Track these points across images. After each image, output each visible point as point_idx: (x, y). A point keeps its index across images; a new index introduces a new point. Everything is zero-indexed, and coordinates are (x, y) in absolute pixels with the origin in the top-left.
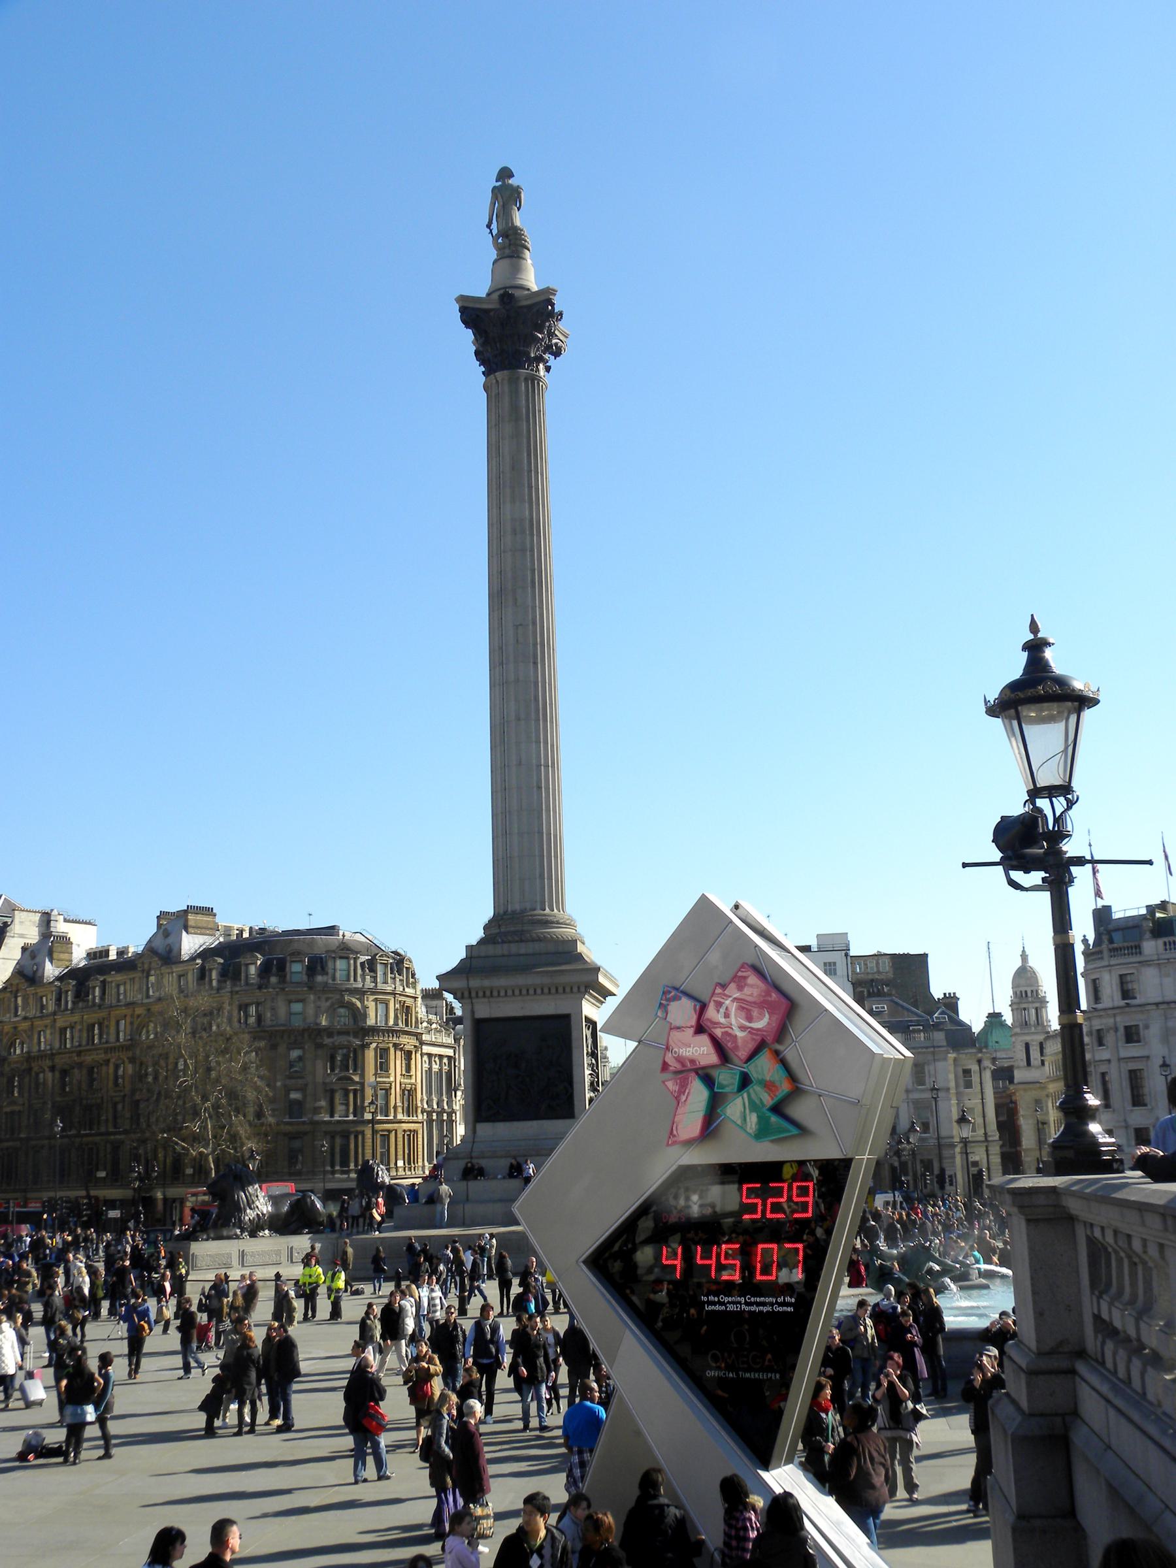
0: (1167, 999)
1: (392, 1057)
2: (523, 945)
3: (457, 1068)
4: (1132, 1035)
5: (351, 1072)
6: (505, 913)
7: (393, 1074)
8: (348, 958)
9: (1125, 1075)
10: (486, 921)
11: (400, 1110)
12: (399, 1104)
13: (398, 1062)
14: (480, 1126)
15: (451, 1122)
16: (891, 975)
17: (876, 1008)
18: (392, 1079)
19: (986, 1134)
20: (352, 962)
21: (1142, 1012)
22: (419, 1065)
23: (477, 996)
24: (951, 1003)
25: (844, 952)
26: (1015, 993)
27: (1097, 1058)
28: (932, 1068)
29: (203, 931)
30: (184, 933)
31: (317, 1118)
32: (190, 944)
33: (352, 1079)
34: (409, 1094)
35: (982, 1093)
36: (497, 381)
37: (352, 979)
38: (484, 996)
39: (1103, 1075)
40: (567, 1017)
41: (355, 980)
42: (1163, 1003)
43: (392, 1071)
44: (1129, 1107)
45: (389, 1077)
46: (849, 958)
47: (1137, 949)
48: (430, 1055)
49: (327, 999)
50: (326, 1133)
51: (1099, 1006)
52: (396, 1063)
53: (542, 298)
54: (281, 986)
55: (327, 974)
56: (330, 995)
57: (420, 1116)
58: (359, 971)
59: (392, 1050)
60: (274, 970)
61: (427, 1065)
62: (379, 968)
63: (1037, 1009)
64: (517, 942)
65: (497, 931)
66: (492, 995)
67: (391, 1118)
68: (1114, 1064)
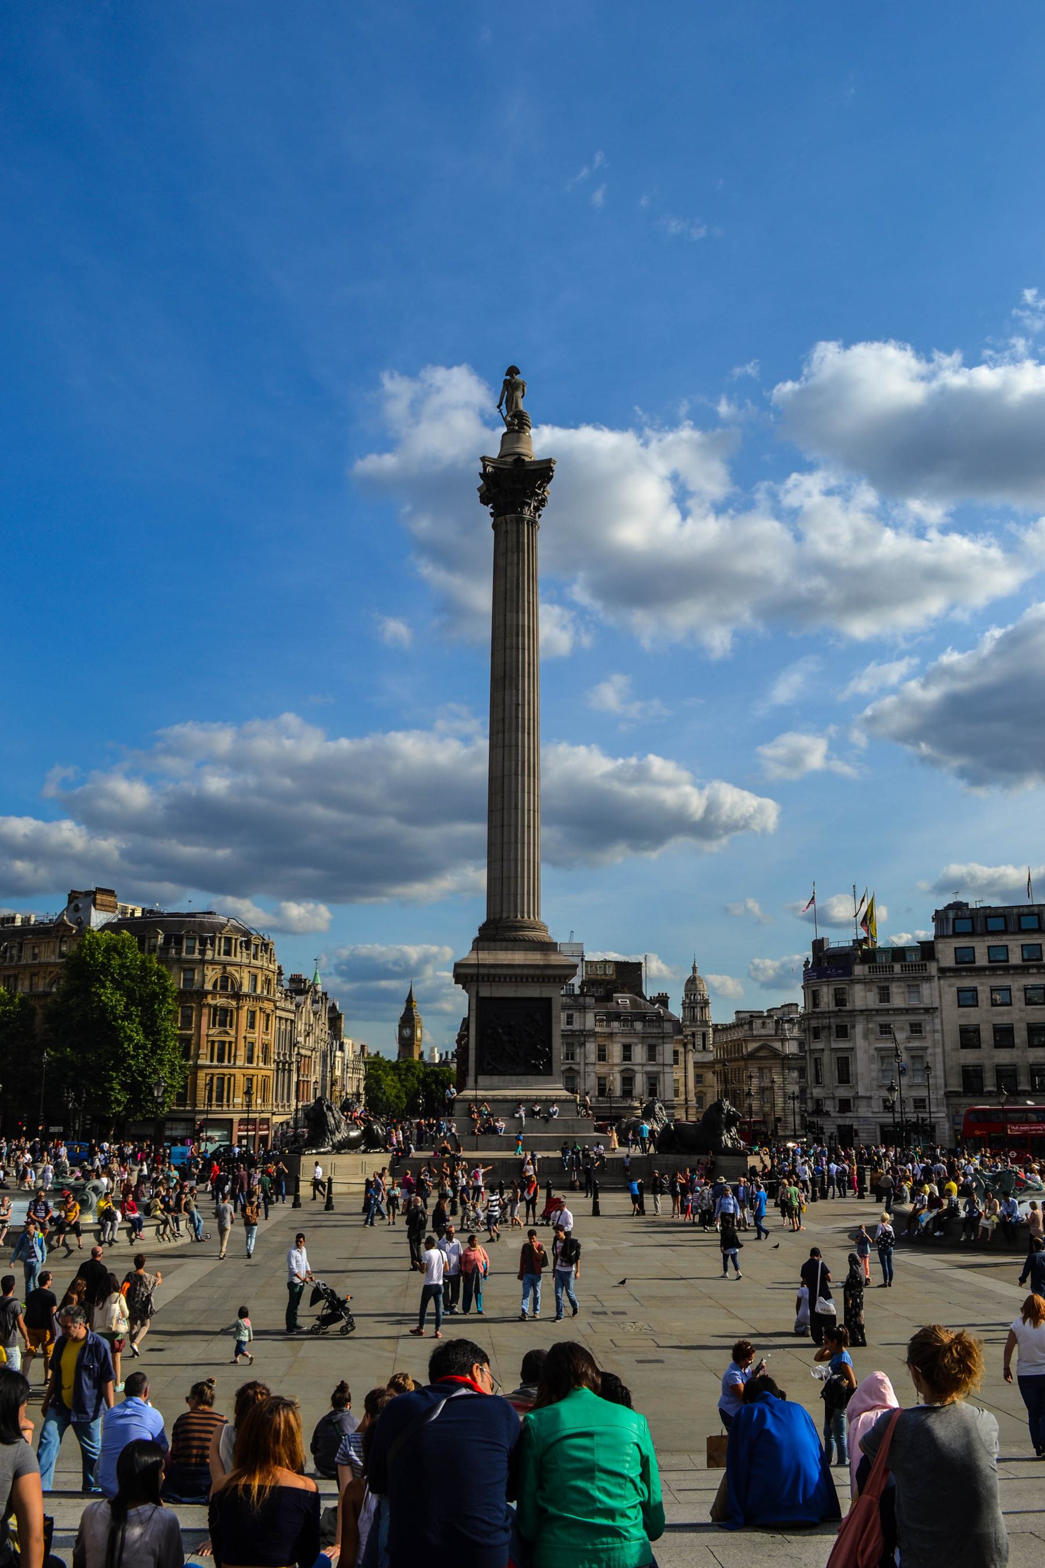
0: (869, 1007)
4: (843, 1032)
6: (501, 918)
9: (834, 1061)
10: (480, 924)
11: (260, 1059)
12: (260, 1055)
13: (262, 1022)
14: (480, 1078)
16: (614, 977)
18: (256, 1035)
19: (686, 1099)
20: (233, 941)
21: (850, 1016)
22: (274, 1023)
23: (483, 981)
24: (663, 1000)
26: (687, 995)
27: (812, 1048)
28: (661, 1048)
29: (107, 908)
30: (93, 909)
31: (200, 1062)
32: (98, 918)
33: (228, 1033)
34: (266, 1048)
35: (686, 1068)
36: (506, 522)
39: (816, 1059)
40: (549, 1000)
41: (235, 956)
42: (866, 1010)
43: (257, 1029)
44: (837, 1084)
45: (254, 1033)
47: (849, 972)
48: (280, 1018)
50: (207, 1075)
51: (818, 1010)
53: (547, 465)
57: (273, 1066)
58: (238, 949)
60: (173, 944)
61: (278, 1026)
62: (253, 947)
63: (702, 1008)
67: (255, 1065)
68: (826, 1053)
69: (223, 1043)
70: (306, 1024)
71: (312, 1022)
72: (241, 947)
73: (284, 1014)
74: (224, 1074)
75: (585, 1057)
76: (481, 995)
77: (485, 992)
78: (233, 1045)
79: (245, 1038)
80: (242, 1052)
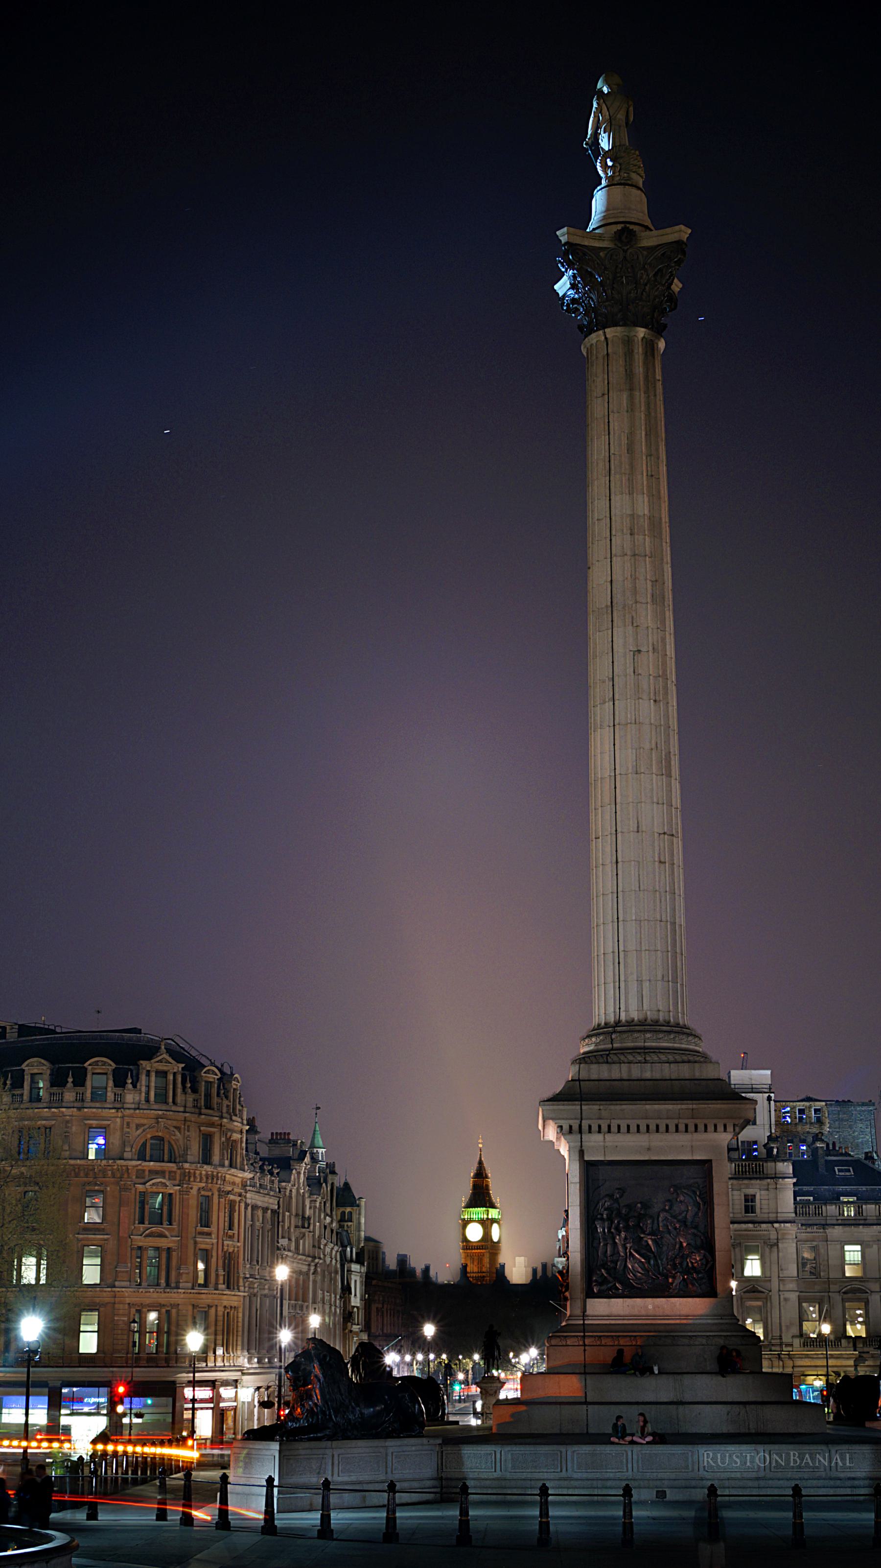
11: (221, 1279)
12: (221, 1272)
13: (222, 1214)
14: (591, 1302)
17: (839, 1171)
20: (171, 1077)
23: (590, 1131)
25: (767, 1095)
37: (171, 1100)
43: (214, 1229)
45: (209, 1234)
46: (772, 1103)
61: (249, 1223)
64: (640, 1062)
66: (609, 1131)
72: (184, 1087)
75: (780, 1269)
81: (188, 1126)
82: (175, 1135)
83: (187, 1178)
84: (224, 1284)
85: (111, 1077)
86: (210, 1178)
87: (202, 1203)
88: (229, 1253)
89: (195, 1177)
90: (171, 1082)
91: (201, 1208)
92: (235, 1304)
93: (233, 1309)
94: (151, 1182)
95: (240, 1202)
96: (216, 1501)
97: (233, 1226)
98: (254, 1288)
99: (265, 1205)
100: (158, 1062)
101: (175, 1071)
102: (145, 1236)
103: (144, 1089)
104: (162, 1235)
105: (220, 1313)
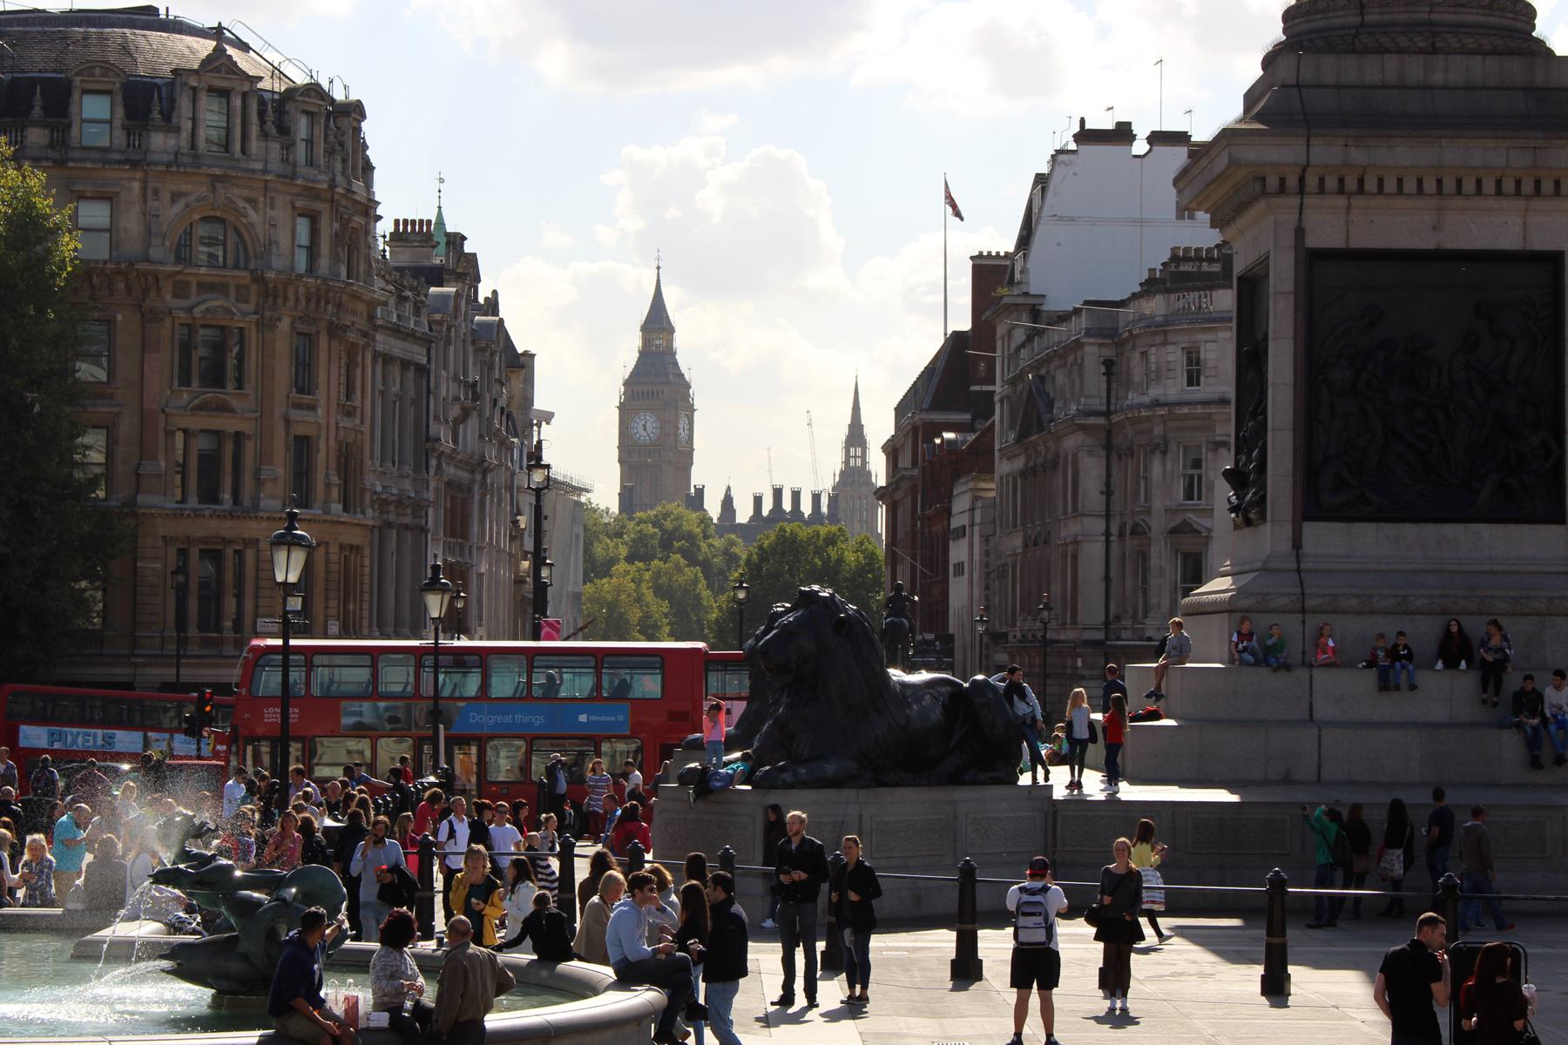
1: (323, 357)
2: (1439, 60)
3: (431, 397)
5: (230, 387)
7: (323, 402)
8: (224, 93)
11: (335, 493)
12: (335, 479)
14: (1311, 530)
15: (423, 530)
22: (369, 375)
23: (1322, 190)
34: (348, 462)
37: (237, 146)
38: (1341, 191)
43: (321, 396)
45: (312, 407)
48: (387, 359)
49: (175, 197)
52: (328, 376)
54: (56, 155)
55: (178, 130)
56: (183, 188)
58: (254, 129)
59: (323, 342)
60: (37, 112)
61: (379, 385)
62: (302, 126)
64: (1422, 51)
65: (1356, 20)
66: (1361, 190)
69: (217, 434)
70: (456, 378)
71: (473, 376)
72: (262, 122)
73: (397, 347)
74: (226, 542)
76: (1314, 241)
77: (1327, 231)
78: (249, 448)
79: (287, 421)
80: (279, 469)
81: (272, 199)
82: (246, 216)
83: (271, 299)
84: (339, 502)
85: (119, 99)
86: (313, 300)
87: (297, 349)
88: (347, 444)
89: (286, 298)
90: (239, 111)
91: (297, 359)
92: (357, 541)
93: (354, 553)
94: (203, 307)
95: (364, 349)
96: (711, 908)
97: (354, 392)
98: (388, 513)
99: (407, 357)
100: (209, 71)
101: (246, 89)
102: (191, 409)
103: (187, 125)
104: (224, 408)
105: (334, 558)
